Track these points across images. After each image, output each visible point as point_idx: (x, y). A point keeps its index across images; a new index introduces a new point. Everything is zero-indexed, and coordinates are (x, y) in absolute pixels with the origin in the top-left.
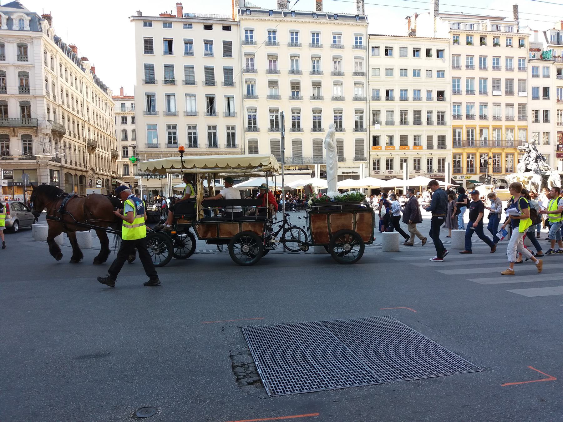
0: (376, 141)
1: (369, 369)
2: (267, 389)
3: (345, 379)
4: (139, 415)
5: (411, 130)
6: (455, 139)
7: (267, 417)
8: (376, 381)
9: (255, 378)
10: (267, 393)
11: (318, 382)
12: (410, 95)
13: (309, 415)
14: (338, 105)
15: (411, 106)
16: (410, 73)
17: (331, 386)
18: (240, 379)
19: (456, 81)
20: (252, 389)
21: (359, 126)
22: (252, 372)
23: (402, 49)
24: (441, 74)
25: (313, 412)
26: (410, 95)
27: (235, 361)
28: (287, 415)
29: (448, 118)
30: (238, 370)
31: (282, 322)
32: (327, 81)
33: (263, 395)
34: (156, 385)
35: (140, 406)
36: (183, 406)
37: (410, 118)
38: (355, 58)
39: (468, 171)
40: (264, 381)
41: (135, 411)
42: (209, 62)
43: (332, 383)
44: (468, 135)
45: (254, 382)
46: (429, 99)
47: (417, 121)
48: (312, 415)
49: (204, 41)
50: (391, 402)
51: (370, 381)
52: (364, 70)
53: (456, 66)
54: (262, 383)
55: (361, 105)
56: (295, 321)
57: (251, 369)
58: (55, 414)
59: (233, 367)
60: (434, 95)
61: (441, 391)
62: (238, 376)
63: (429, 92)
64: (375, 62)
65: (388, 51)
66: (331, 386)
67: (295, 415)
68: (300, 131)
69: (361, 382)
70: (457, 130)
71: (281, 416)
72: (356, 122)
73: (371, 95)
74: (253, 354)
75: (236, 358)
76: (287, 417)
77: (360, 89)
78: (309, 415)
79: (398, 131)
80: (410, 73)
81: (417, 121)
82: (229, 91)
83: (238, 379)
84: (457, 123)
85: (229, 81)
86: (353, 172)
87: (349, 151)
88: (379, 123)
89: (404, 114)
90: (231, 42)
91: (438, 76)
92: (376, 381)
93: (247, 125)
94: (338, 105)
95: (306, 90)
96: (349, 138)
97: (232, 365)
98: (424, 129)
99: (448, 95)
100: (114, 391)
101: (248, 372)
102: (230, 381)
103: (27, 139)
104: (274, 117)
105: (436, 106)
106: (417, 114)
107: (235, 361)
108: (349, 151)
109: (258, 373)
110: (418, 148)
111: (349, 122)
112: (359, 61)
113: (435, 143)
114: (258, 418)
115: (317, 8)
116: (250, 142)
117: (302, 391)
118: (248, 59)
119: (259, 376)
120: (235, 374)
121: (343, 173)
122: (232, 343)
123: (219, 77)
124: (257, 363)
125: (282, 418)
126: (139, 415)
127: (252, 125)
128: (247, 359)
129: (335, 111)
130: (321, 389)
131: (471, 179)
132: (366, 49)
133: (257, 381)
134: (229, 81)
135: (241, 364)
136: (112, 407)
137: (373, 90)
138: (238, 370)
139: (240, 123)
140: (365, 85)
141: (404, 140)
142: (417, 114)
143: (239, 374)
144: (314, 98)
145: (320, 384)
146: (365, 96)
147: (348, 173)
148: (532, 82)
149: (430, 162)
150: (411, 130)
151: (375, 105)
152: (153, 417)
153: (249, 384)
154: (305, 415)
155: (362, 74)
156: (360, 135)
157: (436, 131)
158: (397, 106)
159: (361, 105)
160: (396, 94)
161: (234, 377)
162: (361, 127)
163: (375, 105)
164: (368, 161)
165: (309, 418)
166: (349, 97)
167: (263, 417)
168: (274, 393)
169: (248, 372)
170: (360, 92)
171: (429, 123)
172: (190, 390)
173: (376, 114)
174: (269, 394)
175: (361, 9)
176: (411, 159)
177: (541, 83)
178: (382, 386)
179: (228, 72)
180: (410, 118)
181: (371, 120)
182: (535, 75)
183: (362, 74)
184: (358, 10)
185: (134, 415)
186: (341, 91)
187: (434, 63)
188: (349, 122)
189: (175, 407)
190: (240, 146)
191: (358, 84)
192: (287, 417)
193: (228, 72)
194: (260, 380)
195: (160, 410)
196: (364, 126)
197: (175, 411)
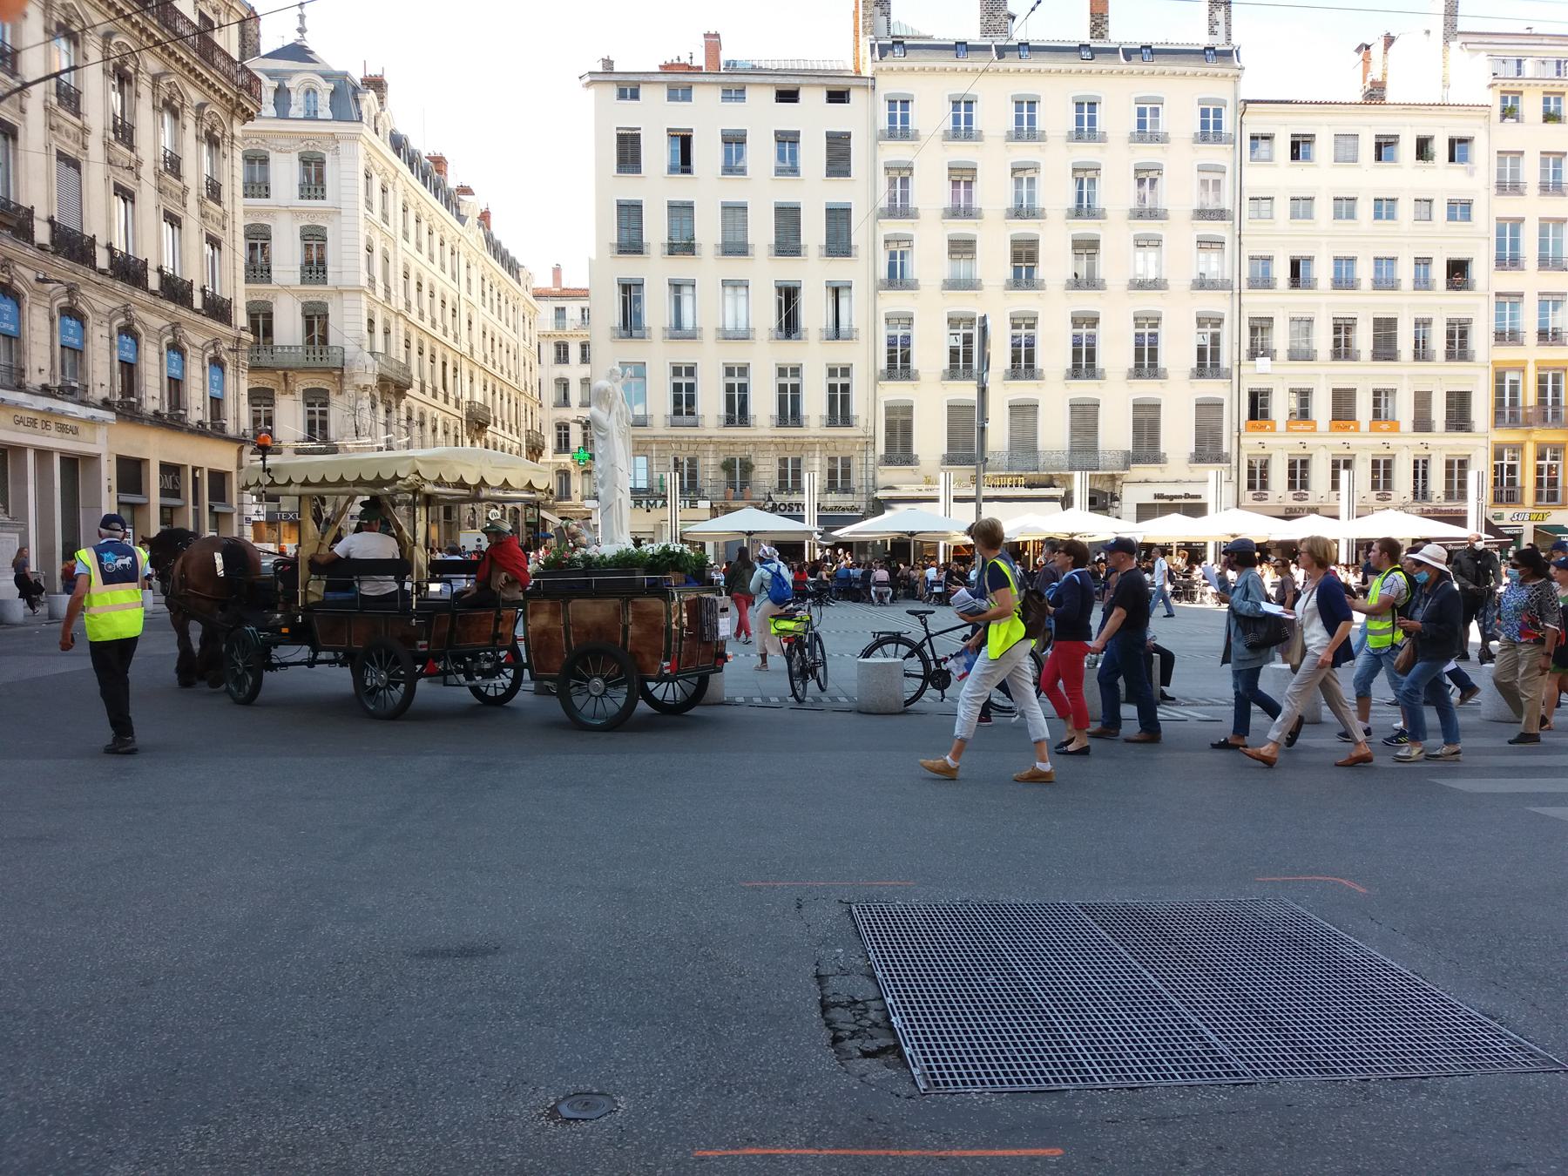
0: (1258, 406)
1: (1216, 1040)
2: (916, 1071)
3: (1143, 1062)
4: (565, 1111)
5: (1364, 375)
6: (1499, 403)
7: (913, 1147)
8: (1236, 1074)
9: (884, 1041)
10: (914, 1082)
11: (1064, 1064)
12: (1364, 272)
13: (1032, 1152)
14: (1148, 302)
15: (1365, 306)
16: (1365, 209)
17: (1101, 1078)
18: (842, 1039)
19: (1508, 231)
20: (876, 1070)
21: (1207, 362)
22: (876, 1025)
23: (1342, 140)
24: (1460, 210)
25: (1047, 1145)
26: (1364, 272)
27: (828, 992)
28: (971, 1148)
29: (1481, 339)
30: (836, 1014)
31: (965, 896)
32: (1115, 235)
33: (904, 1088)
34: (615, 1038)
35: (571, 1088)
36: (684, 1098)
37: (1364, 339)
38: (1201, 169)
39: (1539, 496)
40: (907, 1051)
41: (557, 1101)
42: (787, 191)
43: (1104, 1071)
44: (1542, 391)
45: (881, 1051)
46: (1422, 283)
47: (1385, 348)
48: (1041, 1151)
49: (777, 133)
50: (1281, 1138)
51: (1218, 1074)
52: (1227, 203)
53: (1509, 186)
54: (901, 1055)
55: (1214, 302)
56: (1002, 898)
57: (872, 1015)
58: (352, 1091)
59: (825, 1007)
60: (1439, 272)
61: (1436, 1118)
62: (835, 1030)
63: (1423, 262)
64: (1258, 178)
65: (1299, 148)
66: (1101, 1078)
67: (992, 1148)
68: (1033, 377)
69: (1191, 1075)
70: (1509, 377)
71: (952, 1148)
72: (1201, 352)
73: (1246, 274)
74: (879, 974)
75: (833, 983)
76: (969, 1153)
77: (1214, 256)
78: (1032, 1152)
79: (1324, 377)
80: (1365, 209)
81: (1385, 348)
82: (839, 270)
83: (836, 1040)
84: (1508, 353)
85: (839, 244)
86: (1187, 496)
87: (1177, 435)
88: (1269, 353)
89: (1343, 328)
90: (849, 135)
91: (1451, 217)
92: (1236, 1074)
93: (883, 364)
94: (1148, 302)
95: (1055, 263)
96: (1178, 400)
97: (822, 1001)
98: (1405, 371)
99: (1481, 271)
100: (503, 1046)
101: (863, 1022)
102: (815, 1044)
103: (316, 401)
104: (960, 338)
105: (1443, 305)
106: (1385, 330)
107: (828, 992)
108: (1177, 435)
109: (891, 1028)
110: (1385, 426)
111: (1177, 352)
113: (1439, 412)
114: (889, 1146)
115: (1093, 30)
116: (890, 410)
117: (1017, 1087)
118: (892, 182)
119: (895, 1036)
120: (829, 1024)
121: (1157, 496)
122: (823, 942)
123: (813, 231)
124: (889, 1000)
125: (955, 1153)
126: (565, 1111)
127: (899, 363)
128: (863, 990)
129: (1138, 320)
130: (1071, 1086)
131: (1549, 521)
132: (1234, 142)
133: (888, 1047)
134: (839, 244)
135: (844, 999)
136: (498, 1085)
137: (1252, 258)
138: (836, 1014)
139: (865, 357)
140: (1227, 246)
141: (1343, 403)
142: (1385, 330)
143: (839, 1025)
144: (1077, 283)
145: (1069, 1072)
146: (1227, 276)
147: (1171, 498)
149: (1421, 470)
150: (1364, 375)
151: (1257, 303)
152: (603, 1120)
153: (866, 1054)
154: (1023, 1152)
155: (1220, 215)
156: (1211, 388)
157: (1442, 377)
158: (1323, 305)
159: (1214, 302)
160: (1322, 271)
161: (826, 1035)
162: (1216, 365)
163: (1257, 303)
164: (1234, 463)
165: (1033, 1159)
166: (1179, 281)
167: (902, 1147)
168: (937, 1083)
169: (863, 1022)
170: (1213, 265)
171: (1421, 352)
172: (703, 1057)
173: (1261, 327)
174: (922, 1086)
175: (1221, 29)
176: (1365, 460)
178: (1254, 1091)
179: (838, 217)
180: (1364, 339)
181: (1246, 345)
183: (1220, 215)
184: (1212, 32)
185: (554, 1112)
186: (1158, 264)
187: (1441, 179)
188: (1177, 352)
189: (661, 1099)
190: (861, 422)
191: (1205, 243)
192: (969, 1153)
193: (838, 217)
194: (898, 1046)
195: (623, 1103)
196: (1225, 362)
197: (661, 1109)
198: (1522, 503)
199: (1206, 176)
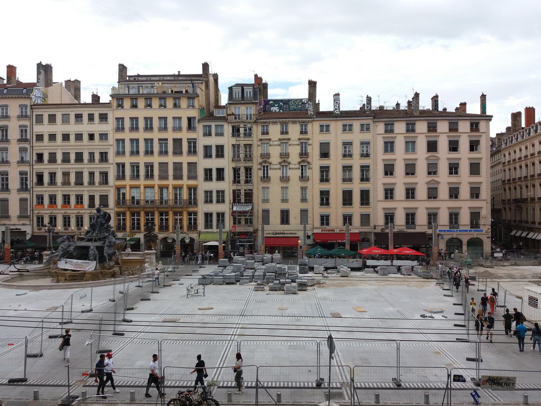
5: (73, 191)
6: (119, 198)
15: (73, 167)
16: (72, 138)
21: (24, 187)
23: (65, 116)
24: (104, 136)
26: (73, 157)
38: (20, 126)
47: (79, 182)
53: (120, 128)
55: (26, 168)
60: (97, 157)
63: (92, 155)
70: (122, 191)
79: (59, 192)
80: (72, 138)
81: (79, 182)
86: (16, 229)
99: (111, 156)
105: (98, 167)
112: (24, 129)
140: (29, 150)
141: (66, 198)
148: (202, 141)
151: (38, 168)
156: (25, 195)
159: (26, 168)
162: (26, 187)
163: (38, 168)
177: (213, 141)
181: (35, 180)
182: (207, 134)
183: (26, 140)
187: (97, 128)
196: (29, 187)
198: (126, 231)
199: (22, 128)
